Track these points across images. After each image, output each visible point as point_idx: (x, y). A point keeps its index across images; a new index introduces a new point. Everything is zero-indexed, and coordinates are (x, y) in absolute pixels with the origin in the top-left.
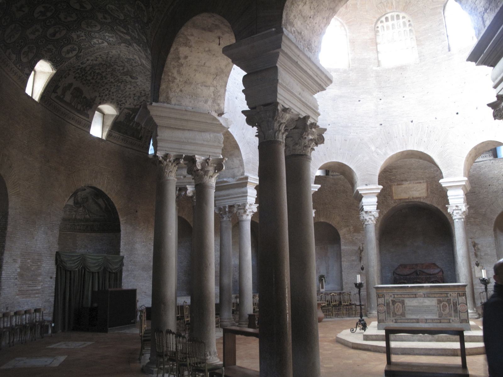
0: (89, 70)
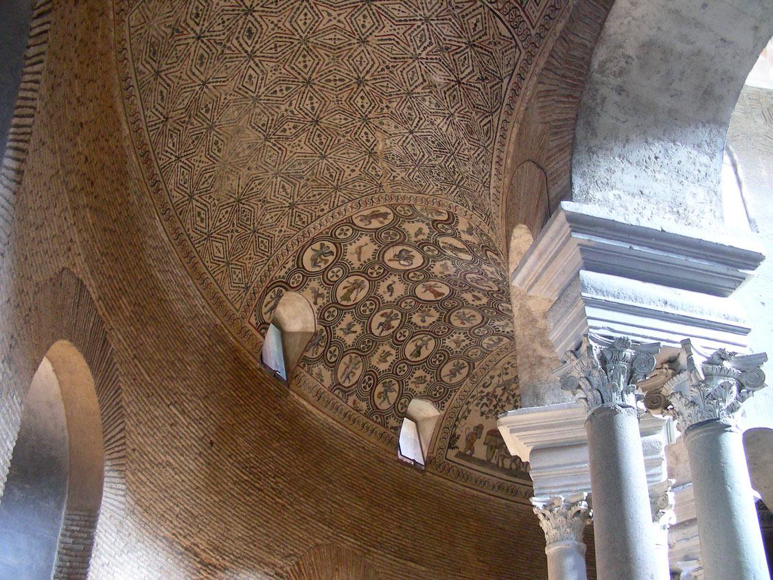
0: (502, 395)
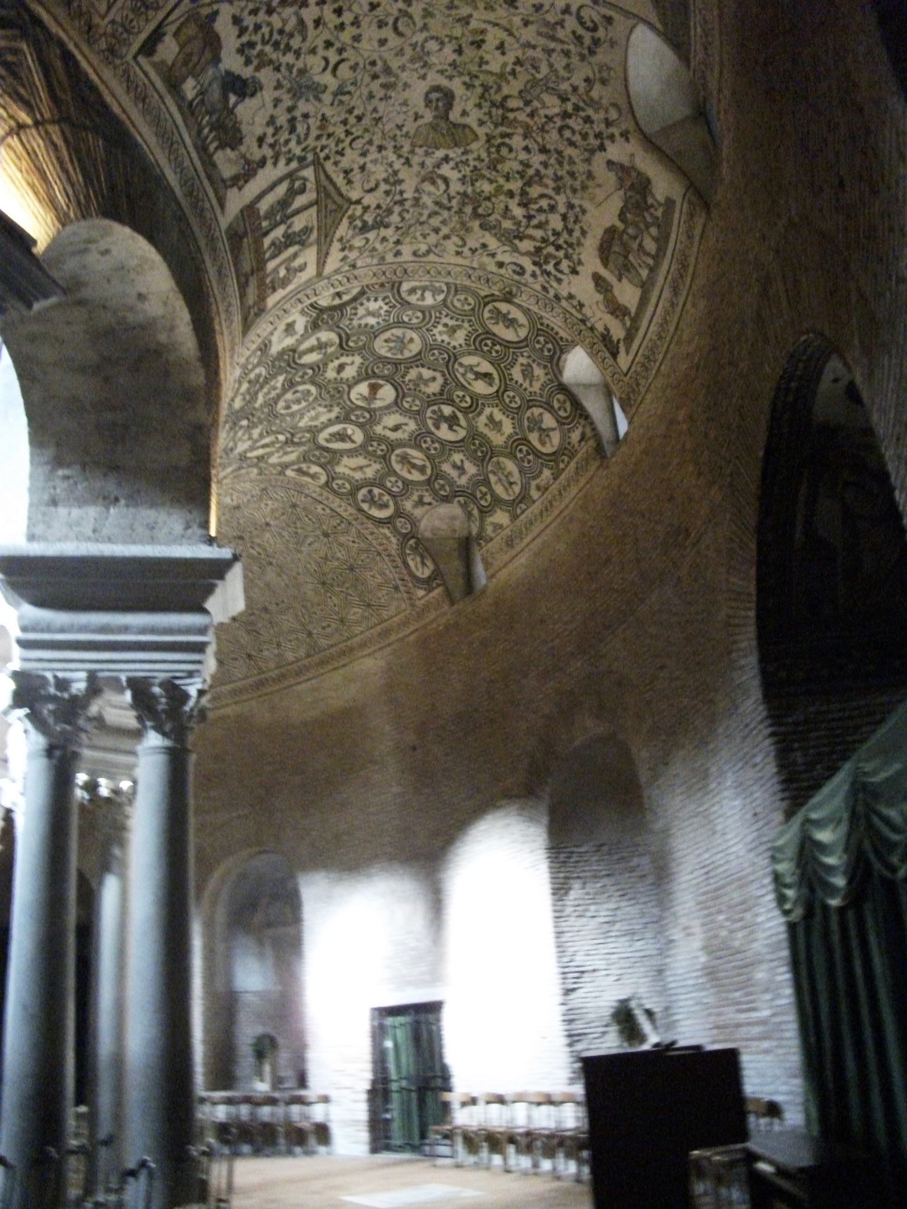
0: (531, 238)
